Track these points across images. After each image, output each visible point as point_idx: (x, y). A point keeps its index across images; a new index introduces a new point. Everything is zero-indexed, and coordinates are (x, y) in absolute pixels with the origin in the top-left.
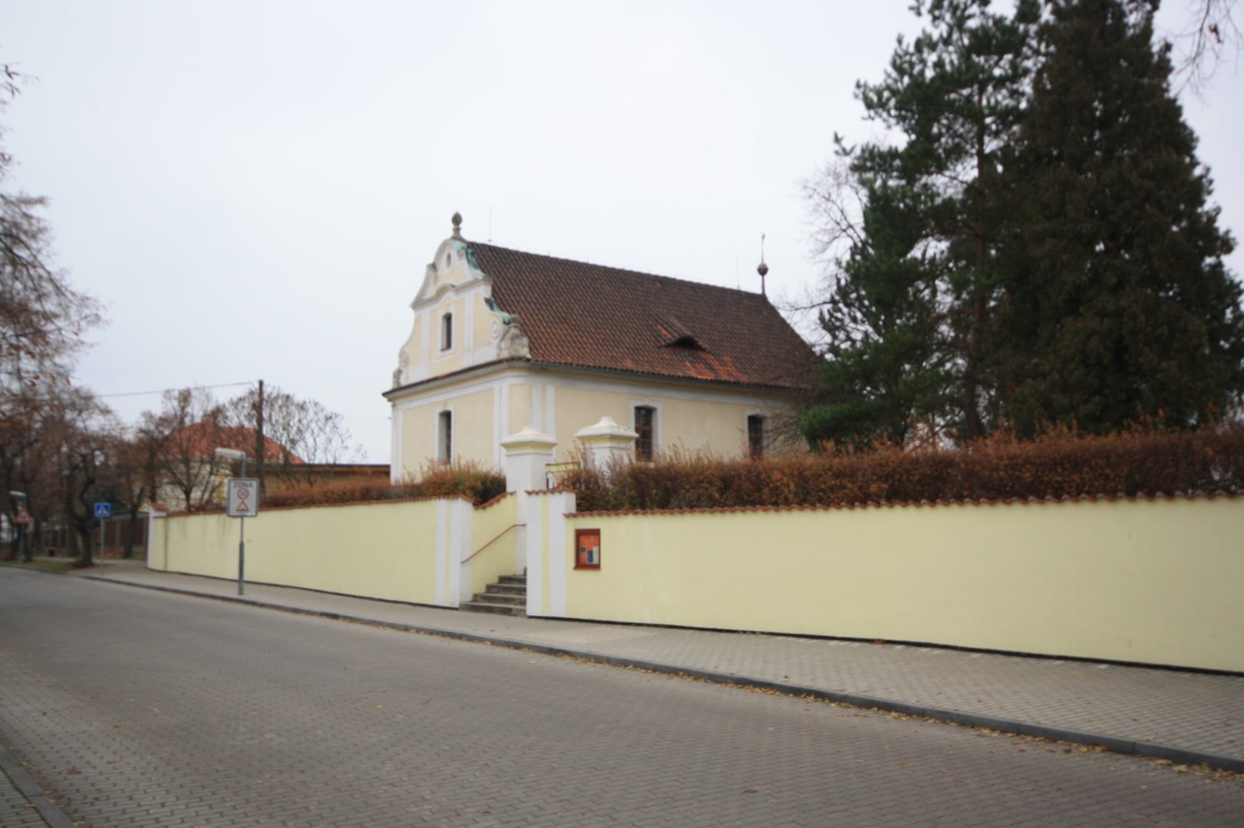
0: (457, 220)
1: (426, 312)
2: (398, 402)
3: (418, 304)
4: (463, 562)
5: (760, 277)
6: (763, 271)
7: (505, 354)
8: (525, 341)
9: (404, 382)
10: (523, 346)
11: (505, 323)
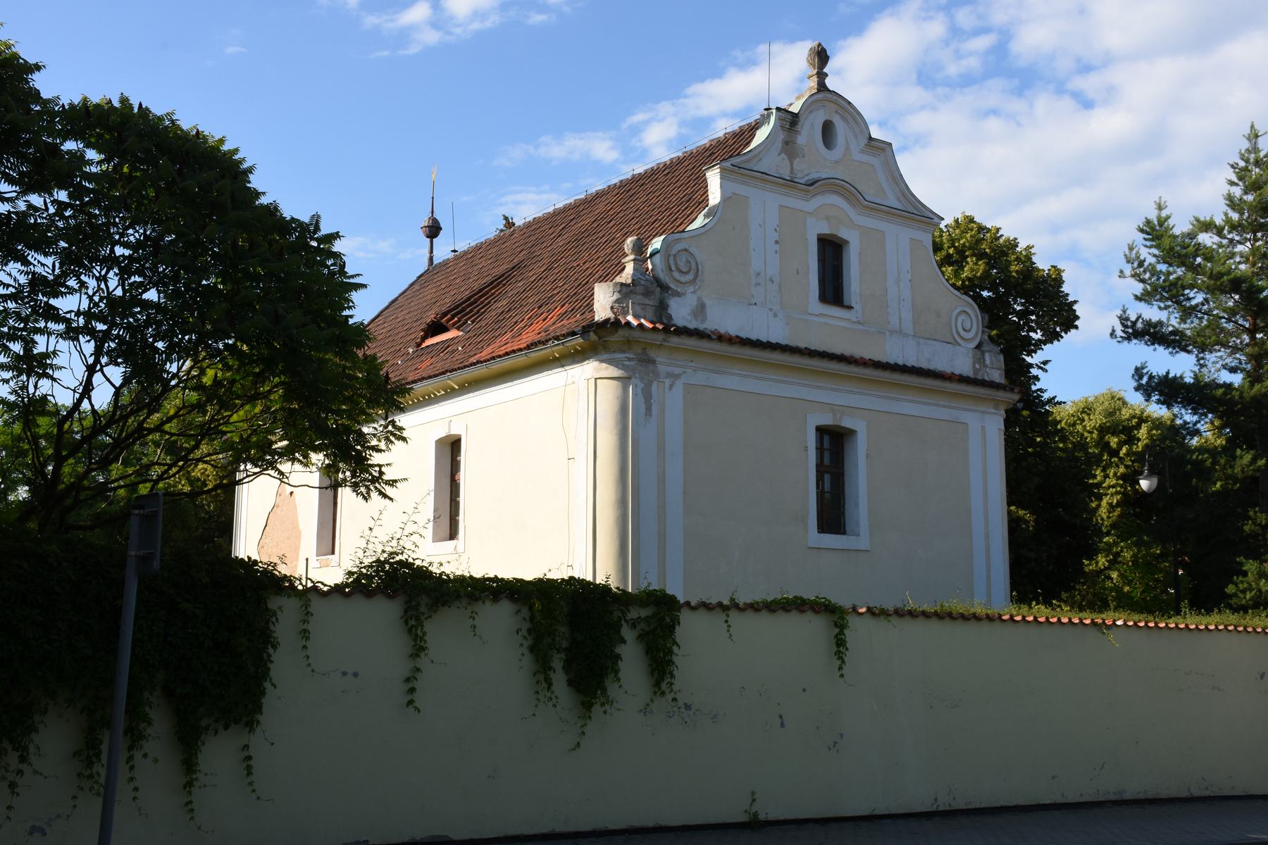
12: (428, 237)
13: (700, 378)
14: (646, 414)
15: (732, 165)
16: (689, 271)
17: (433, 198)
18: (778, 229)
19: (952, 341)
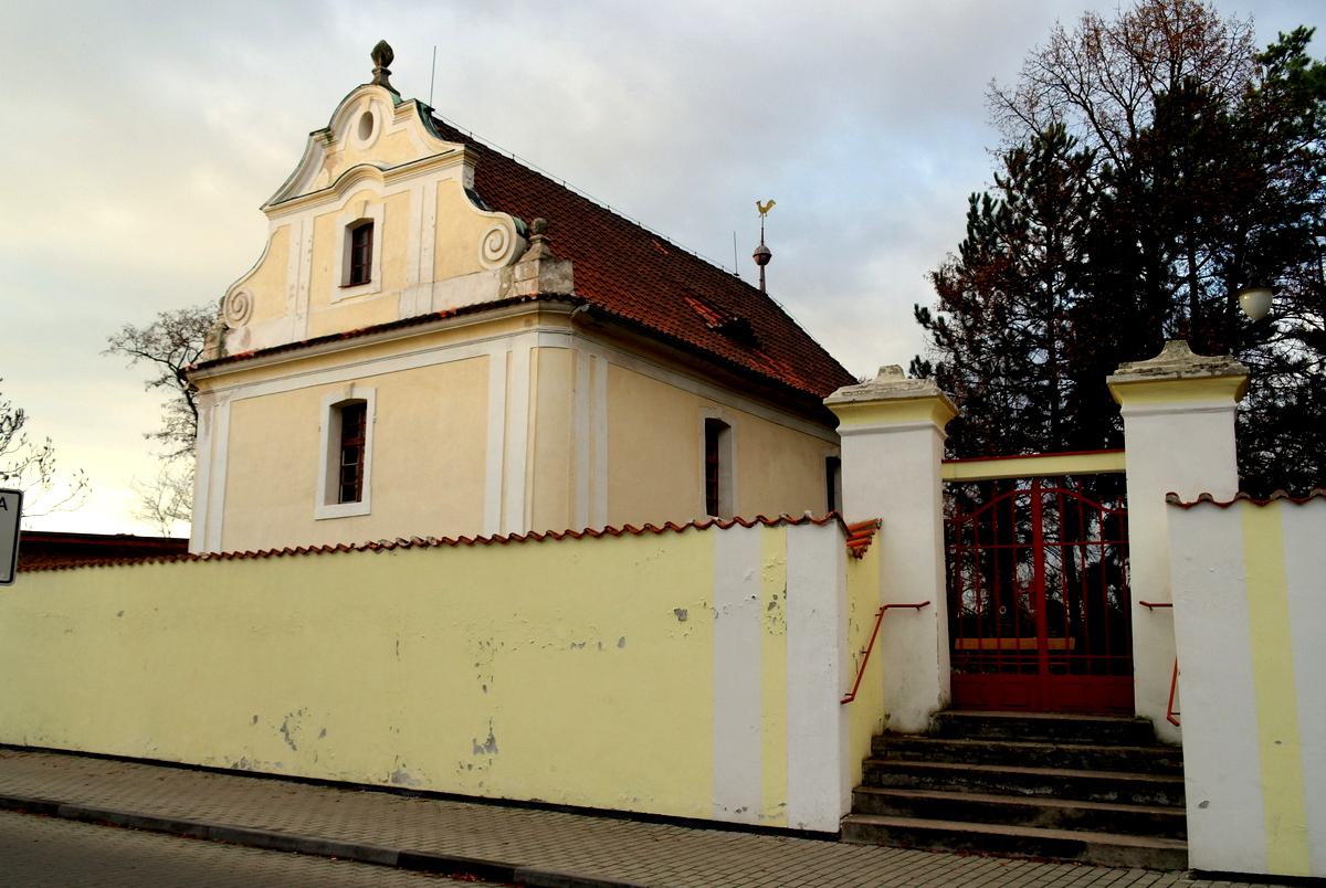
0: (383, 55)
1: (301, 222)
2: (215, 386)
3: (285, 200)
4: (843, 702)
5: (759, 267)
6: (763, 258)
7: (528, 288)
8: (568, 268)
9: (234, 347)
10: (564, 277)
11: (519, 232)
13: (245, 392)
19: (480, 269)
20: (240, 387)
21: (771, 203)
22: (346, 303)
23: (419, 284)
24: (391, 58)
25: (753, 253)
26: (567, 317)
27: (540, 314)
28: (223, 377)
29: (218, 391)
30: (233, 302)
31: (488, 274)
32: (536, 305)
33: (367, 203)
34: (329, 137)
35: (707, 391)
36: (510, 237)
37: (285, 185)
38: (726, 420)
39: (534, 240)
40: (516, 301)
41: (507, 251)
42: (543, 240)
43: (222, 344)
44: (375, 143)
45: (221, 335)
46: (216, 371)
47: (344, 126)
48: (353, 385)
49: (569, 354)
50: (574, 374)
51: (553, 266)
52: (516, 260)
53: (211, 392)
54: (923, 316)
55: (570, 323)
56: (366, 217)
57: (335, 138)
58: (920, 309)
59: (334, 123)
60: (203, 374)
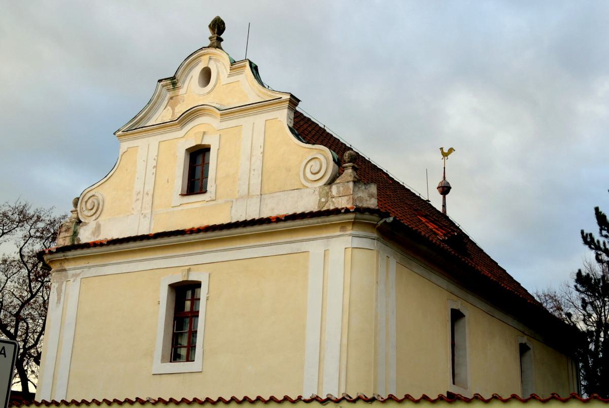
2: (67, 266)
5: (442, 196)
6: (445, 189)
7: (343, 203)
8: (373, 189)
9: (85, 236)
10: (371, 196)
11: (334, 160)
12: (441, 194)
13: (93, 272)
14: (57, 303)
15: (123, 132)
16: (92, 209)
17: (444, 168)
18: (156, 158)
20: (90, 267)
21: (451, 150)
22: (186, 207)
23: (249, 195)
24: (224, 29)
25: (437, 186)
26: (374, 226)
27: (355, 223)
28: (75, 259)
29: (70, 269)
30: (86, 202)
31: (308, 190)
32: (351, 216)
33: (204, 133)
34: (174, 84)
35: (453, 288)
36: (328, 164)
37: (135, 117)
38: (463, 311)
39: (347, 167)
40: (337, 212)
41: (325, 173)
42: (354, 168)
43: (75, 233)
44: (212, 90)
45: (75, 227)
46: (70, 254)
47: (186, 76)
48: (189, 270)
49: (375, 253)
50: (377, 268)
51: (363, 187)
52: (331, 182)
53: (65, 270)
54: (588, 240)
55: (375, 231)
56: (203, 143)
57: (179, 84)
58: (585, 234)
59: (179, 73)
60: (60, 256)
